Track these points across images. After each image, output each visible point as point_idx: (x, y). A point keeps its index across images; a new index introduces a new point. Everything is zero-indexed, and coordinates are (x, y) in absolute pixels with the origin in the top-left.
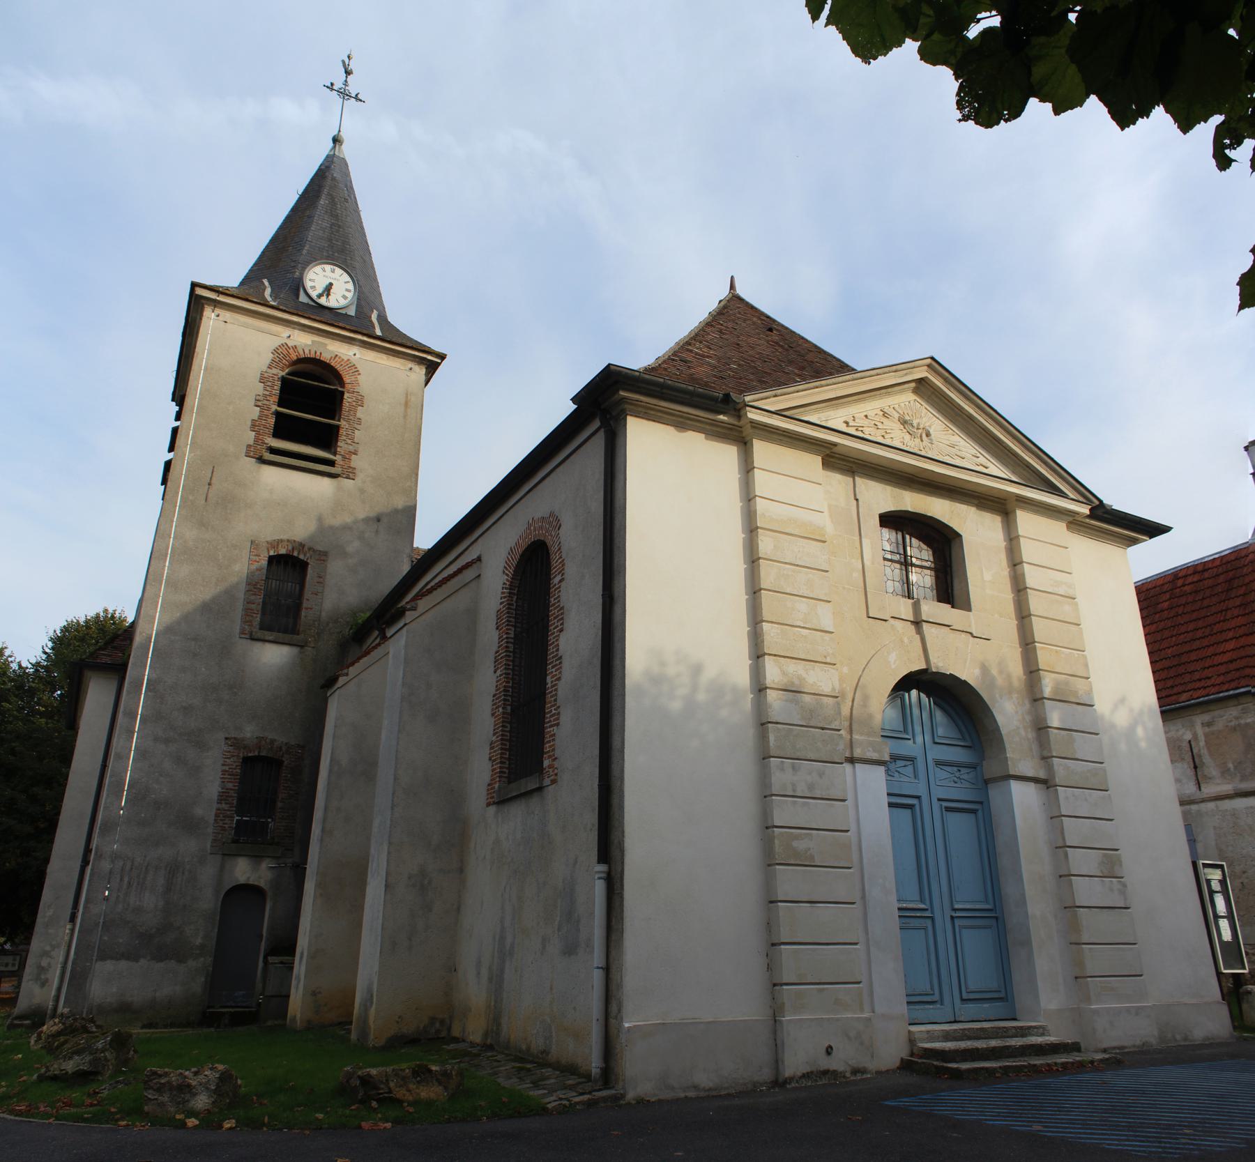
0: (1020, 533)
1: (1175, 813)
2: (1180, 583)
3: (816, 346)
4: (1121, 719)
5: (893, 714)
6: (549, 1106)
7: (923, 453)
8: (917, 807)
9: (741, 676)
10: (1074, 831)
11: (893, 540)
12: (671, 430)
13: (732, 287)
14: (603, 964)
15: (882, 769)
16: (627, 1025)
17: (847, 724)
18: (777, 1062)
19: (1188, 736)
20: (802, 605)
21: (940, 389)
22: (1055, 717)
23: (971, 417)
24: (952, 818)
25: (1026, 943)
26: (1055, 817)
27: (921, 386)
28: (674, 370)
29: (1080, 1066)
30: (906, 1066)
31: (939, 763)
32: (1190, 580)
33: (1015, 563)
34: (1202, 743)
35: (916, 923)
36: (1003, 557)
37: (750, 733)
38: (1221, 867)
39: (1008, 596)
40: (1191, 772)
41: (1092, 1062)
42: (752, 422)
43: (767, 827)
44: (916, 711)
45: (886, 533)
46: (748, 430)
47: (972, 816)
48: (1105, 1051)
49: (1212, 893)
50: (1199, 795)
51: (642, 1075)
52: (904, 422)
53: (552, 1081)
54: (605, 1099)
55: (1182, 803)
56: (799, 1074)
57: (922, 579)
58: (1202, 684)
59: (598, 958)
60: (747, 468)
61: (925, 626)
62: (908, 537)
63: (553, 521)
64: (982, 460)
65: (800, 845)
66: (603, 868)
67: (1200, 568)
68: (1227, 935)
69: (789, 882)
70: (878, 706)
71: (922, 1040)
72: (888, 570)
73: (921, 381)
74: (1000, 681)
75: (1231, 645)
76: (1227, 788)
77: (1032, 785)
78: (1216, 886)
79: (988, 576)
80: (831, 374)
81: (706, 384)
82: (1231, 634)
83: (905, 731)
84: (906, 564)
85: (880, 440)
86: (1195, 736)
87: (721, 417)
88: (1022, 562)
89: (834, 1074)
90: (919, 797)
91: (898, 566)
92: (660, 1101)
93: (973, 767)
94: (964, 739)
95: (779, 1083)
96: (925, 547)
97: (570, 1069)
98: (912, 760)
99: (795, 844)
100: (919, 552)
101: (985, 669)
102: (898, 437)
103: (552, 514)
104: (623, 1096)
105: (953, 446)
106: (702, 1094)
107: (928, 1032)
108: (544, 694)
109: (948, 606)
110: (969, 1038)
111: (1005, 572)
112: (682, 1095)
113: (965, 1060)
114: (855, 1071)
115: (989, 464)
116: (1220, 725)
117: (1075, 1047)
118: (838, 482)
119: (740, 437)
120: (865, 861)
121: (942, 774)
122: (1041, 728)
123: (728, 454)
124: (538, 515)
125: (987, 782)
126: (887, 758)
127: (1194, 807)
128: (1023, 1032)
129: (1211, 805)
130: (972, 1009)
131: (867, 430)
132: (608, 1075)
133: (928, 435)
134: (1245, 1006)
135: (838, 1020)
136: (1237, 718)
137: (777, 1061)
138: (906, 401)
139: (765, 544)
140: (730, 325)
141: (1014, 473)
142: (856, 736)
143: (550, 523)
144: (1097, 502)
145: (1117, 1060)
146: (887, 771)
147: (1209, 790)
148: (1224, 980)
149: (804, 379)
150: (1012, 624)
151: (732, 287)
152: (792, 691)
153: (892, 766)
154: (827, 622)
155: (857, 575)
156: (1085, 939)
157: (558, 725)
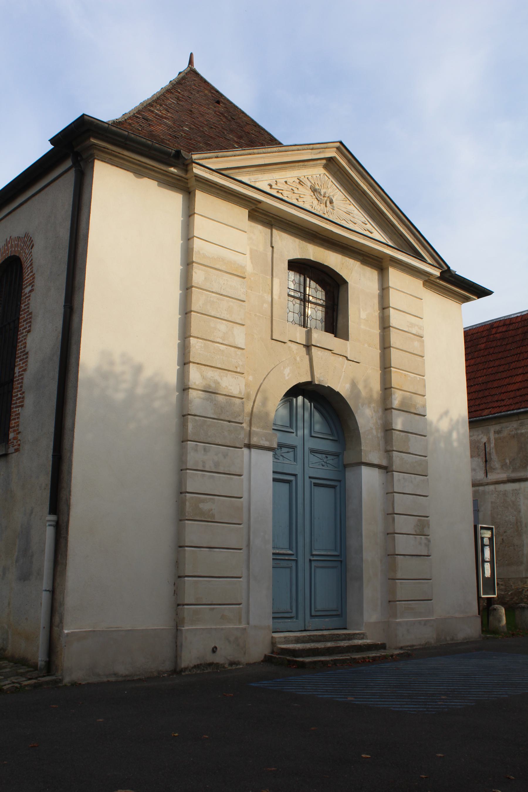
0: (391, 284)
1: (468, 491)
2: (494, 331)
3: (252, 121)
4: (444, 426)
5: (284, 412)
6: (5, 688)
7: (326, 216)
10: (401, 503)
11: (297, 281)
12: (130, 175)
13: (191, 62)
14: (49, 588)
15: (271, 454)
16: (66, 631)
17: (247, 419)
18: (176, 657)
19: (484, 440)
20: (223, 327)
21: (344, 168)
22: (399, 422)
23: (364, 193)
24: (318, 491)
25: (360, 578)
26: (389, 493)
27: (330, 164)
28: (136, 126)
29: (385, 657)
30: (268, 660)
31: (313, 451)
32: (500, 329)
33: (384, 306)
34: (492, 445)
36: (376, 301)
37: (173, 422)
38: (491, 529)
39: (376, 331)
40: (482, 465)
41: (392, 656)
42: (197, 176)
43: (181, 492)
44: (300, 411)
45: (292, 275)
46: (192, 182)
47: (332, 490)
48: (401, 648)
49: (483, 546)
50: (485, 480)
51: (75, 665)
52: (314, 190)
53: (8, 670)
54: (47, 683)
55: (474, 485)
56: (192, 665)
57: (315, 313)
58: (499, 404)
59: (46, 583)
60: (189, 213)
61: (314, 349)
62: (308, 280)
63: (27, 241)
64: (369, 226)
65: (205, 507)
66: (53, 518)
67: (508, 322)
68: (488, 574)
69: (194, 532)
70: (274, 406)
71: (281, 643)
72: (291, 304)
73: (331, 160)
74: (364, 393)
75: (519, 378)
76: (503, 476)
78: (486, 541)
79: (363, 315)
80: (262, 145)
81: (162, 141)
82: (520, 371)
83: (291, 426)
84: (304, 300)
85: (295, 202)
86: (489, 440)
87: (172, 169)
88: (389, 307)
89: (217, 665)
90: (295, 475)
91: (298, 301)
92: (88, 684)
93: (336, 455)
94: (332, 435)
95: (176, 671)
96: (319, 288)
97: (21, 662)
99: (201, 506)
100: (315, 292)
101: (354, 385)
102: (308, 201)
103: (27, 235)
104: (61, 681)
105: (348, 213)
106: (120, 679)
107: (285, 637)
108: (12, 381)
109: (332, 336)
110: (313, 641)
111: (376, 313)
112: (105, 680)
113: (309, 656)
114: (231, 664)
115: (373, 230)
116: (505, 433)
117: (383, 646)
118: (259, 231)
119: (186, 187)
121: (314, 459)
122: (387, 430)
123: (175, 200)
124: (15, 235)
125: (345, 466)
126: (275, 446)
127: (481, 488)
128: (350, 637)
129: (492, 487)
130: (317, 622)
131: (285, 193)
132: (50, 666)
133: (331, 202)
134: (491, 618)
135: (222, 629)
136: (516, 429)
137: (176, 657)
138: (318, 174)
139: (198, 276)
140: (186, 94)
141: (391, 239)
142: (254, 429)
143: (25, 243)
144: (446, 268)
145: (409, 654)
146: (275, 456)
147: (493, 477)
148: (481, 601)
149: (241, 146)
150: (376, 352)
151: (191, 62)
152: (210, 392)
153: (278, 452)
154: (240, 341)
155: (267, 306)
156: (399, 576)
157: (22, 406)
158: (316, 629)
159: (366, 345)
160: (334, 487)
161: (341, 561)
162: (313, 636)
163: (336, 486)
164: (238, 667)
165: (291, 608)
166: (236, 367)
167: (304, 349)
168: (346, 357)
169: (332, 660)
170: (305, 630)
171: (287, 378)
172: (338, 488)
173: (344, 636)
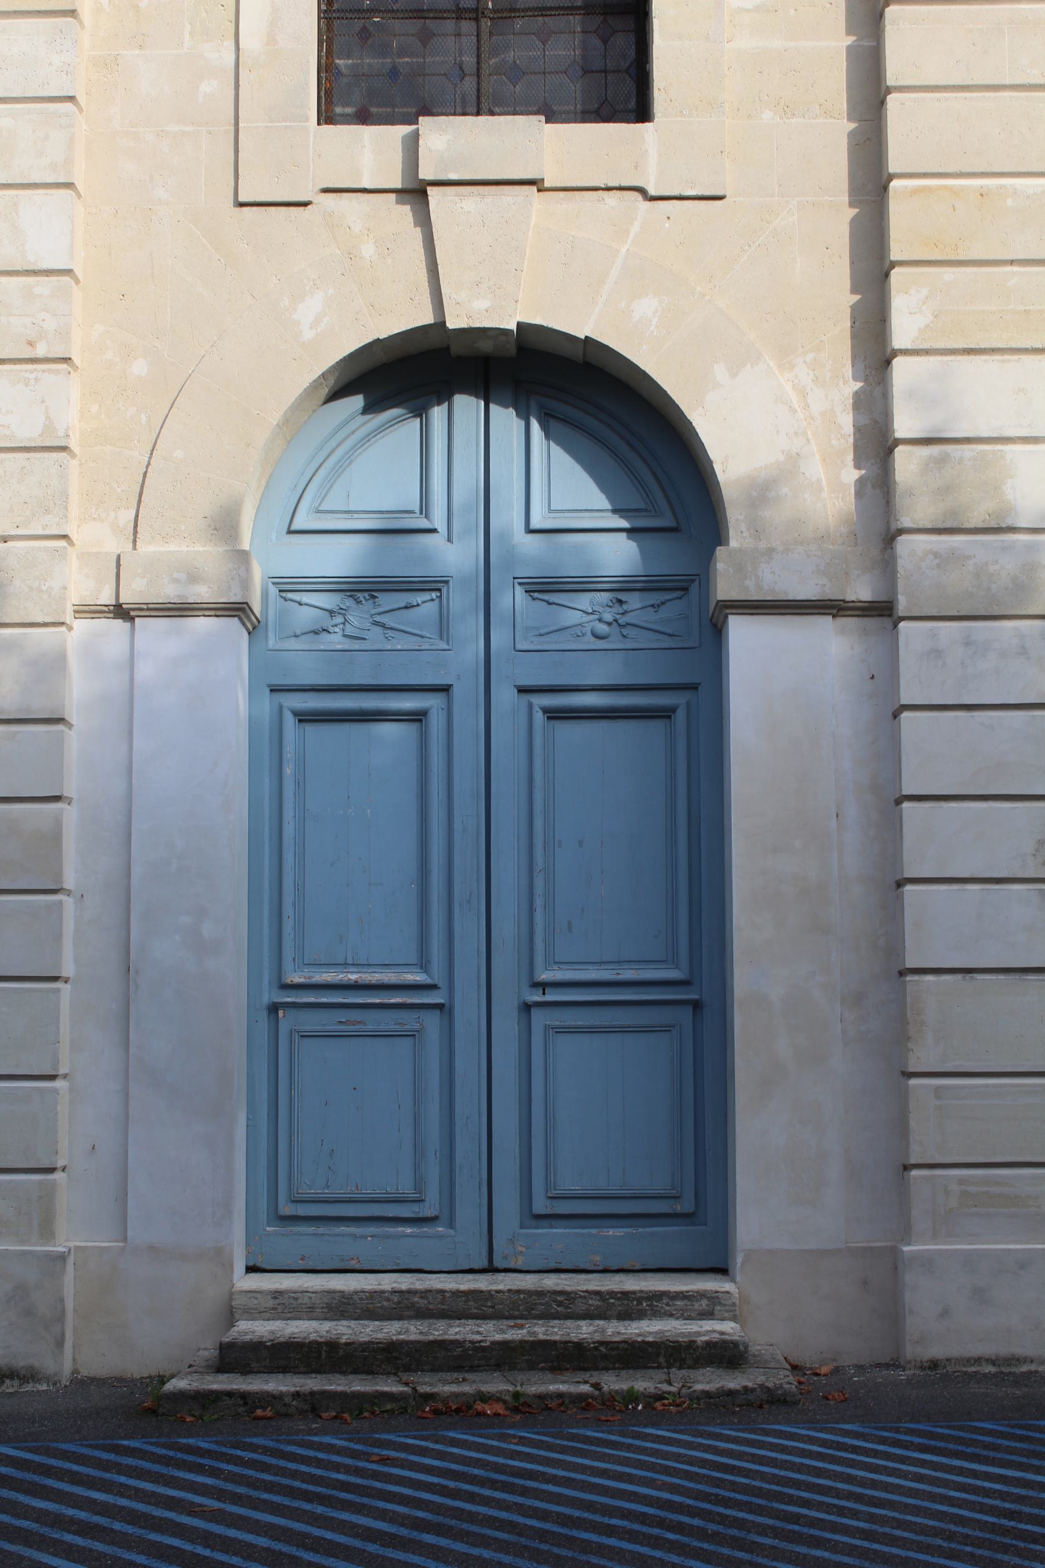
8: (436, 722)
9: (493, 407)
35: (387, 1021)
71: (253, 1313)
77: (825, 623)
90: (445, 689)
98: (435, 585)
107: (277, 1294)
120: (137, 871)
155: (214, 89)
158: (553, 1265)
159: (767, 115)
160: (664, 714)
161: (697, 1006)
162: (425, 1293)
163: (673, 710)
164: (29, 1387)
165: (419, 1184)
166: (31, 344)
167: (405, 212)
168: (641, 191)
169: (297, 1395)
170: (491, 1269)
171: (308, 335)
172: (680, 716)
173: (595, 1302)
